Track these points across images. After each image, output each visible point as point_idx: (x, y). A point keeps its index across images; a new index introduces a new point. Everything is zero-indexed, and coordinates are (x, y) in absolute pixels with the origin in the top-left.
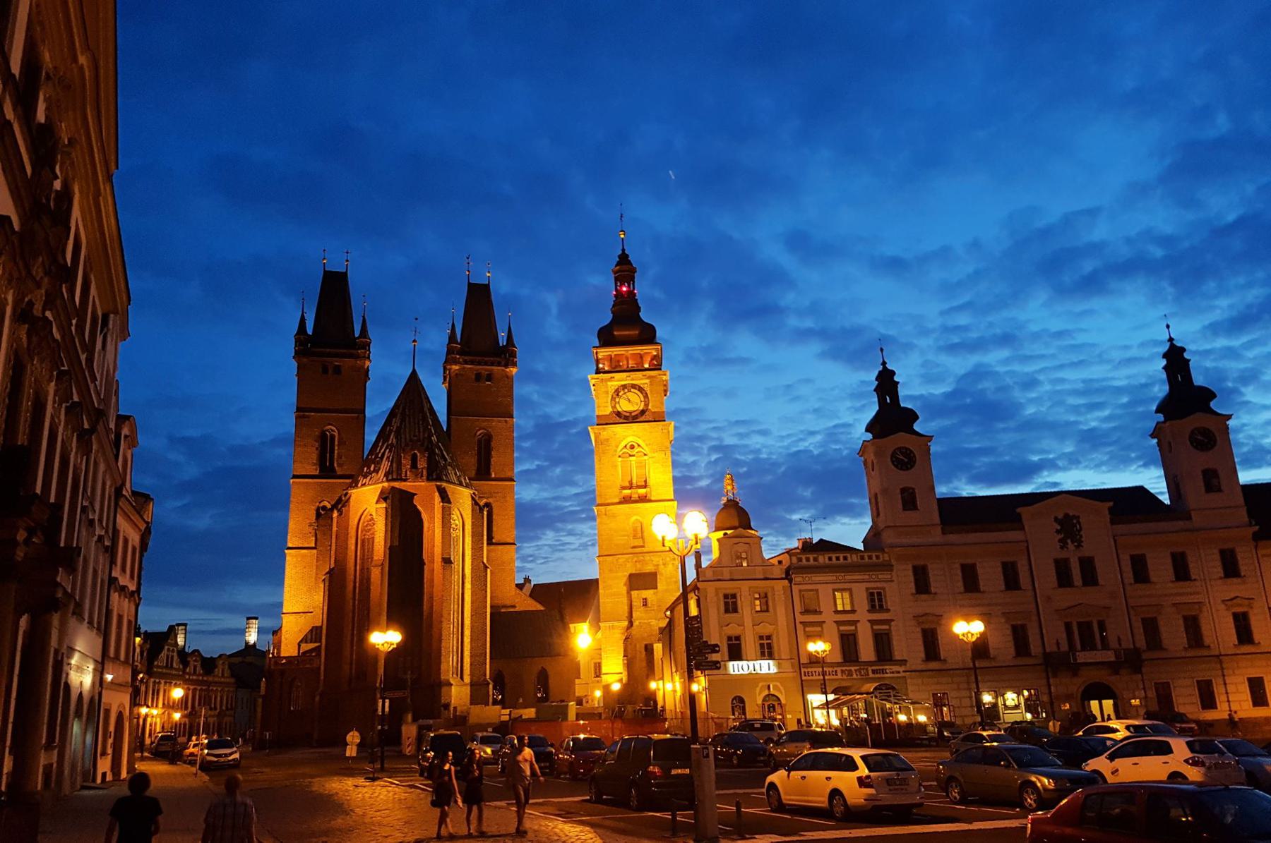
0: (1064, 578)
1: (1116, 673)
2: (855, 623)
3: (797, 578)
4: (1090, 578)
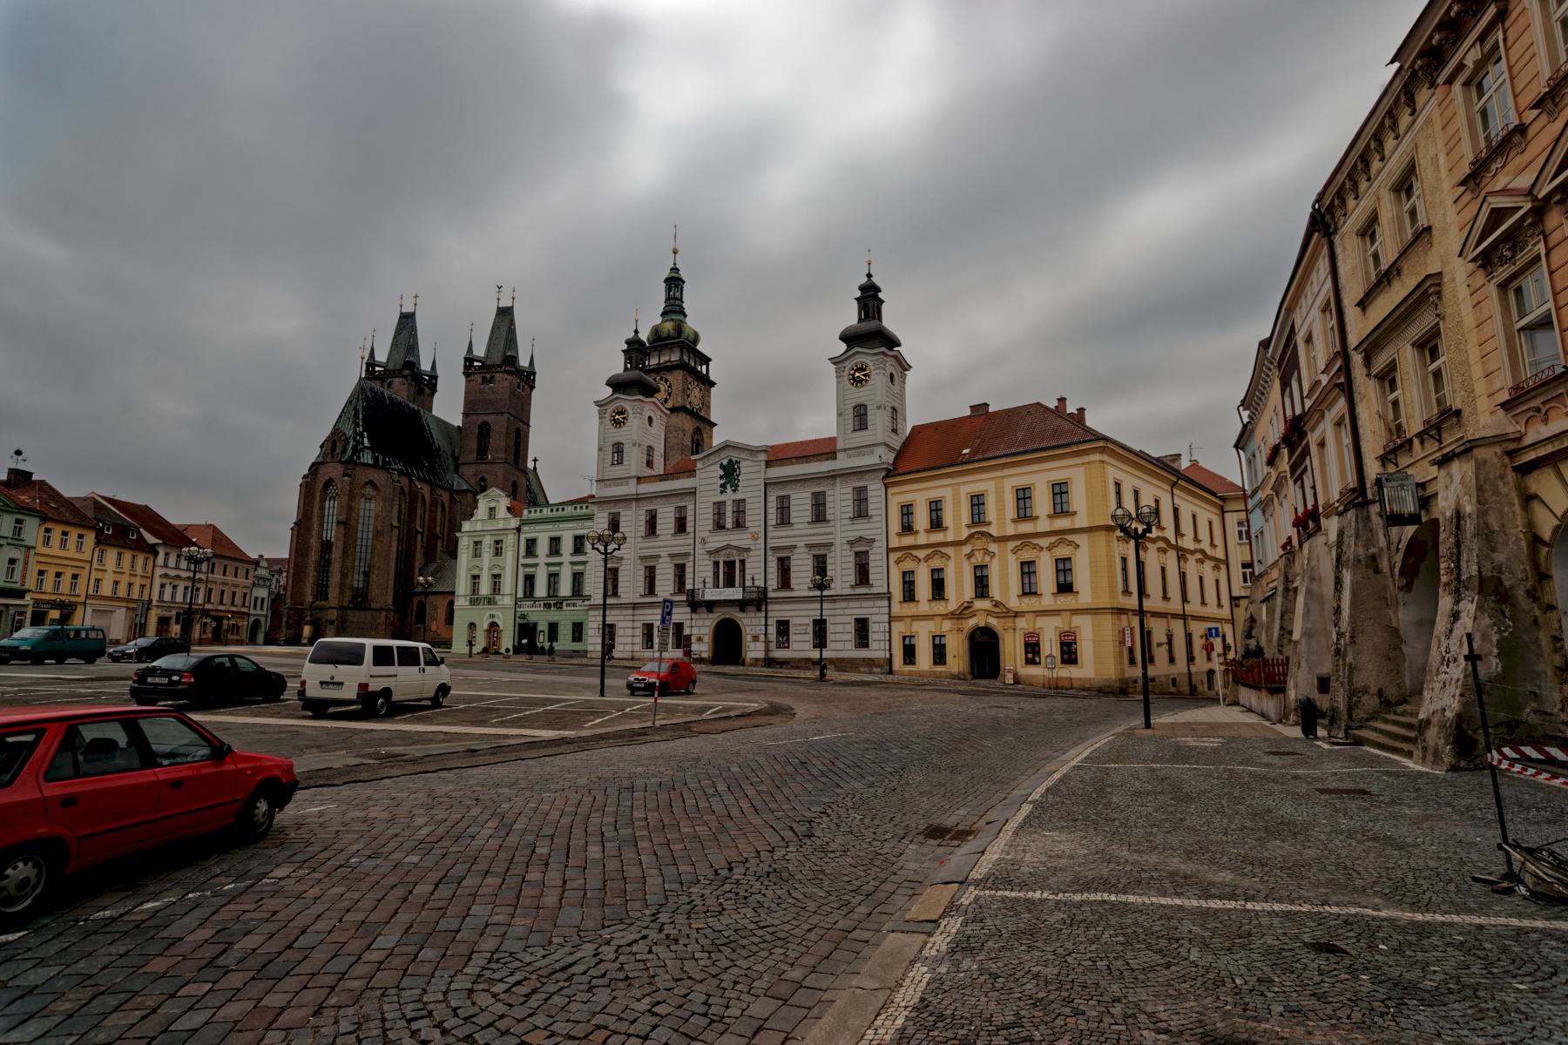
0: (719, 526)
1: (743, 610)
2: (560, 564)
3: (525, 528)
4: (739, 524)
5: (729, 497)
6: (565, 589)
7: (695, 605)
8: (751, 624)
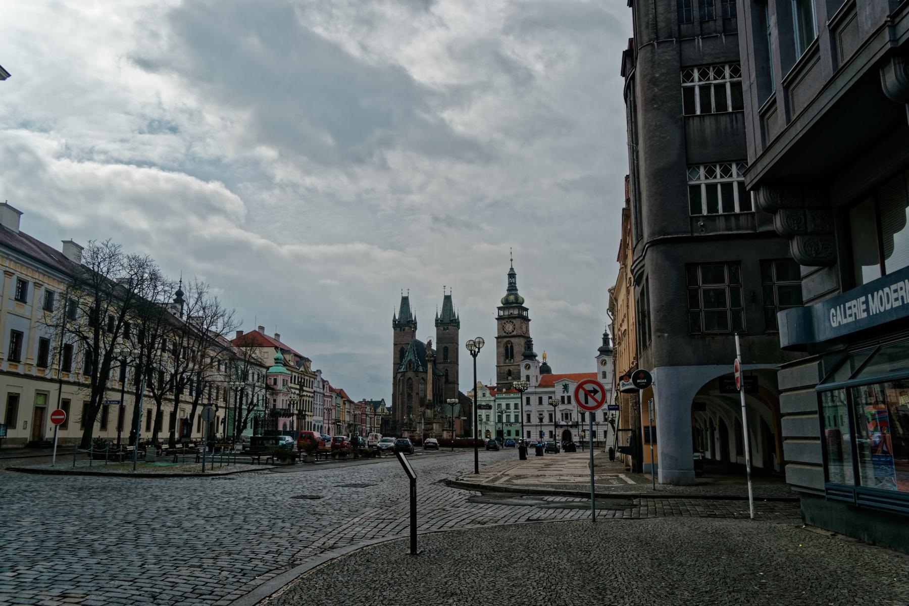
4: (569, 402)
5: (566, 395)
6: (512, 420)
7: (557, 426)
8: (574, 432)
